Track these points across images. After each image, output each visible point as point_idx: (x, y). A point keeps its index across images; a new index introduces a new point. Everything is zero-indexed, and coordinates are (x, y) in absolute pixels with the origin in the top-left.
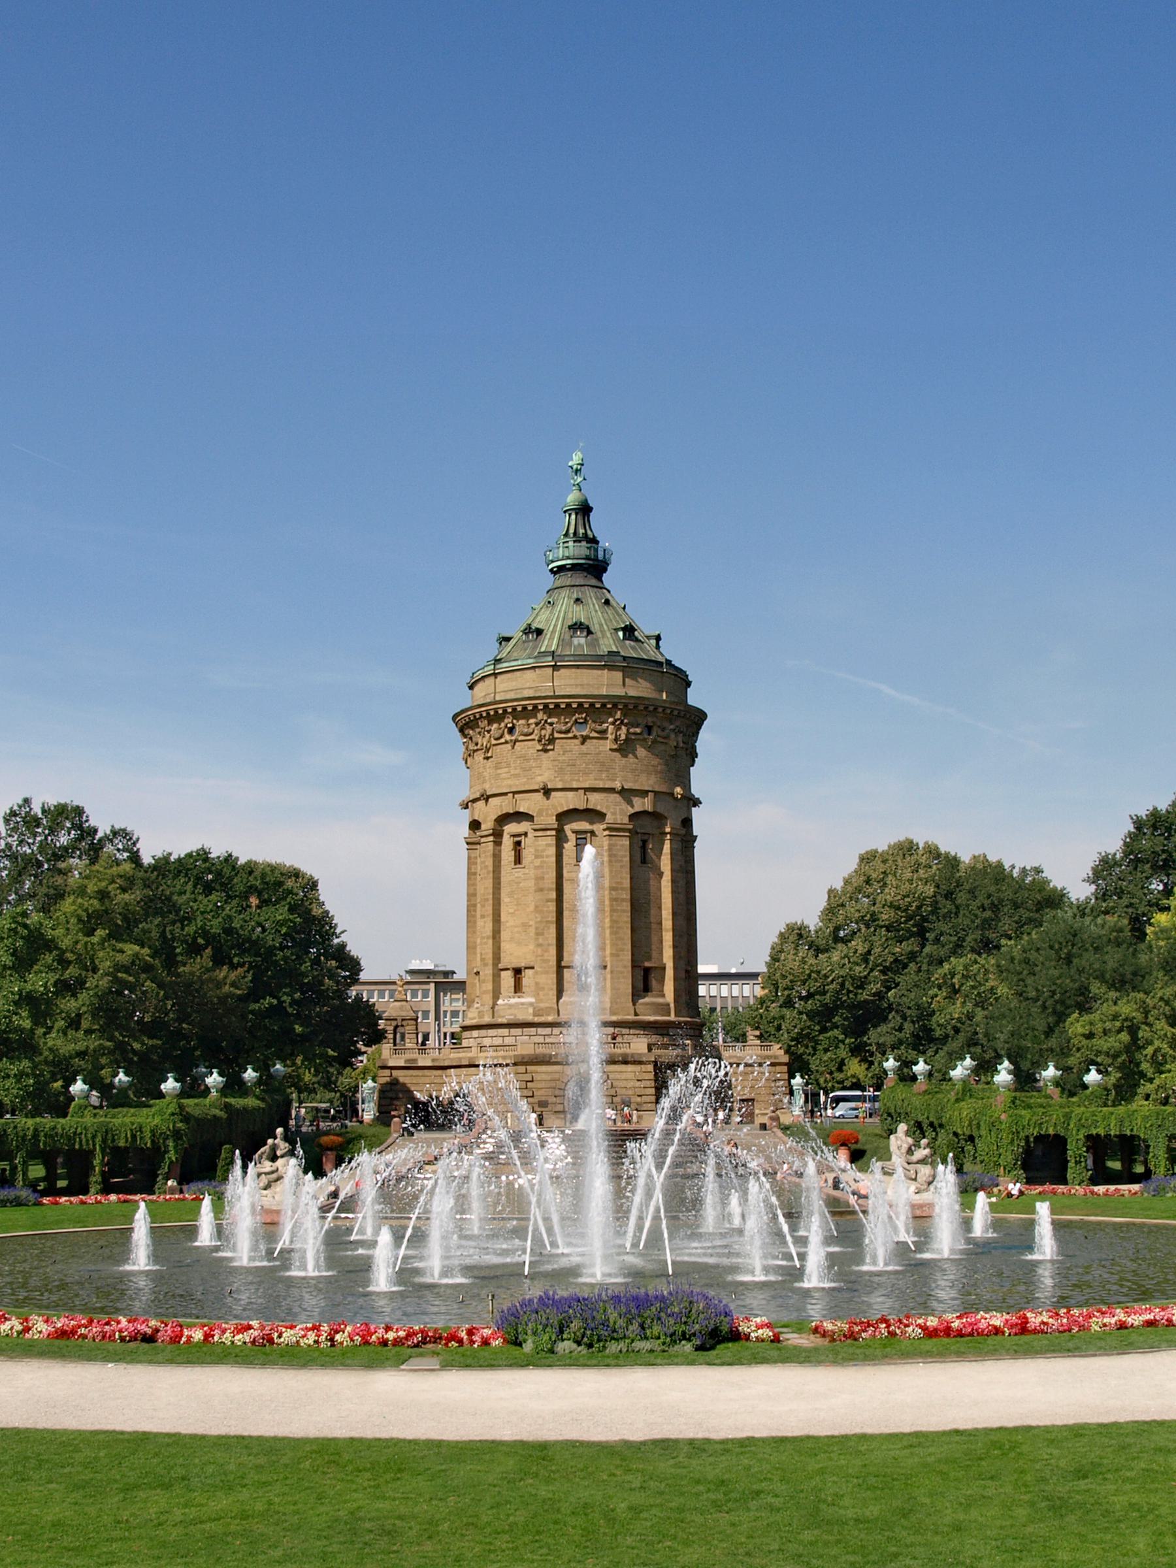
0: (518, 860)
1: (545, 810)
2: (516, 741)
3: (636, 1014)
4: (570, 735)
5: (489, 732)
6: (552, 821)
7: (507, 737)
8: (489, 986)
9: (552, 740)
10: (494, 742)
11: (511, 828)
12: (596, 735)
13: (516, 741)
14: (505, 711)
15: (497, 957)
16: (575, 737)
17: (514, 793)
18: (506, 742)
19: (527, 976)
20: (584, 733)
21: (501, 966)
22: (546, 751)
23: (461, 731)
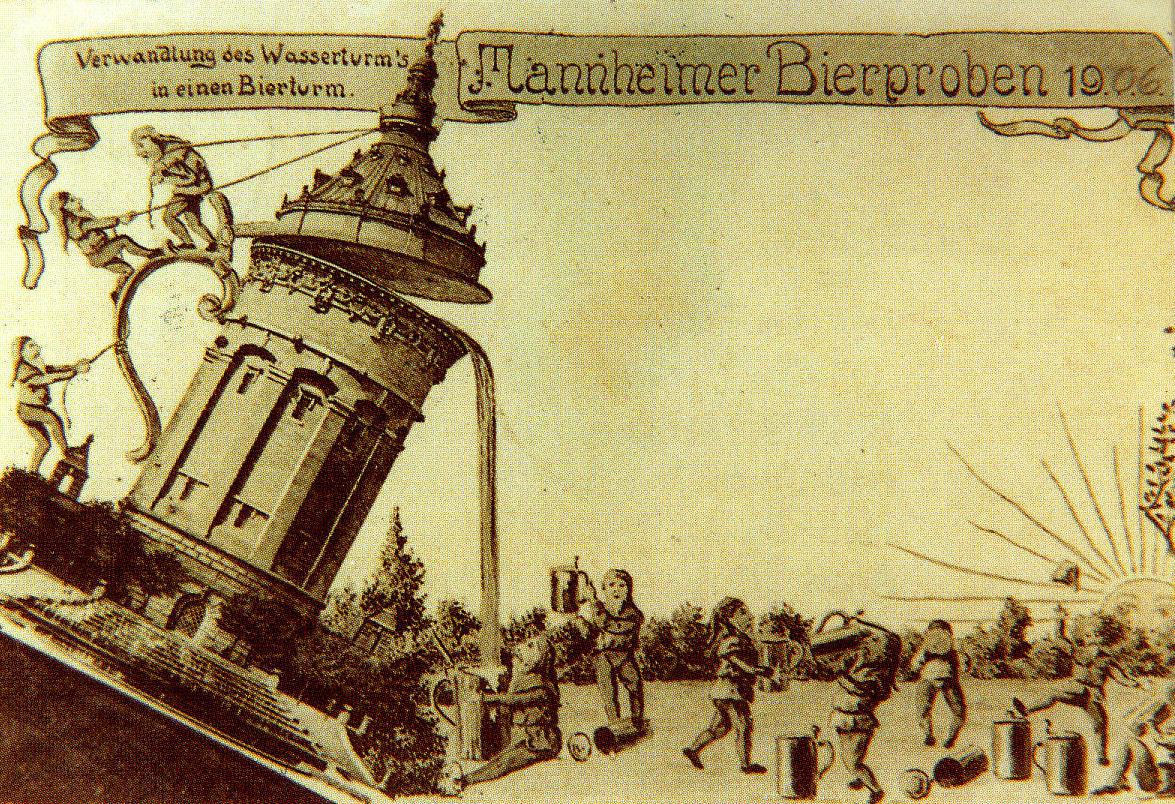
0: (242, 390)
1: (288, 362)
2: (296, 290)
3: (273, 569)
4: (344, 308)
5: (278, 270)
6: (291, 371)
7: (291, 283)
8: (161, 482)
9: (328, 306)
10: (276, 280)
11: (251, 360)
12: (367, 319)
13: (296, 290)
14: (300, 260)
15: (181, 461)
16: (348, 312)
17: (270, 332)
18: (287, 286)
19: (197, 489)
20: (359, 313)
21: (180, 470)
22: (318, 312)
23: (254, 256)
